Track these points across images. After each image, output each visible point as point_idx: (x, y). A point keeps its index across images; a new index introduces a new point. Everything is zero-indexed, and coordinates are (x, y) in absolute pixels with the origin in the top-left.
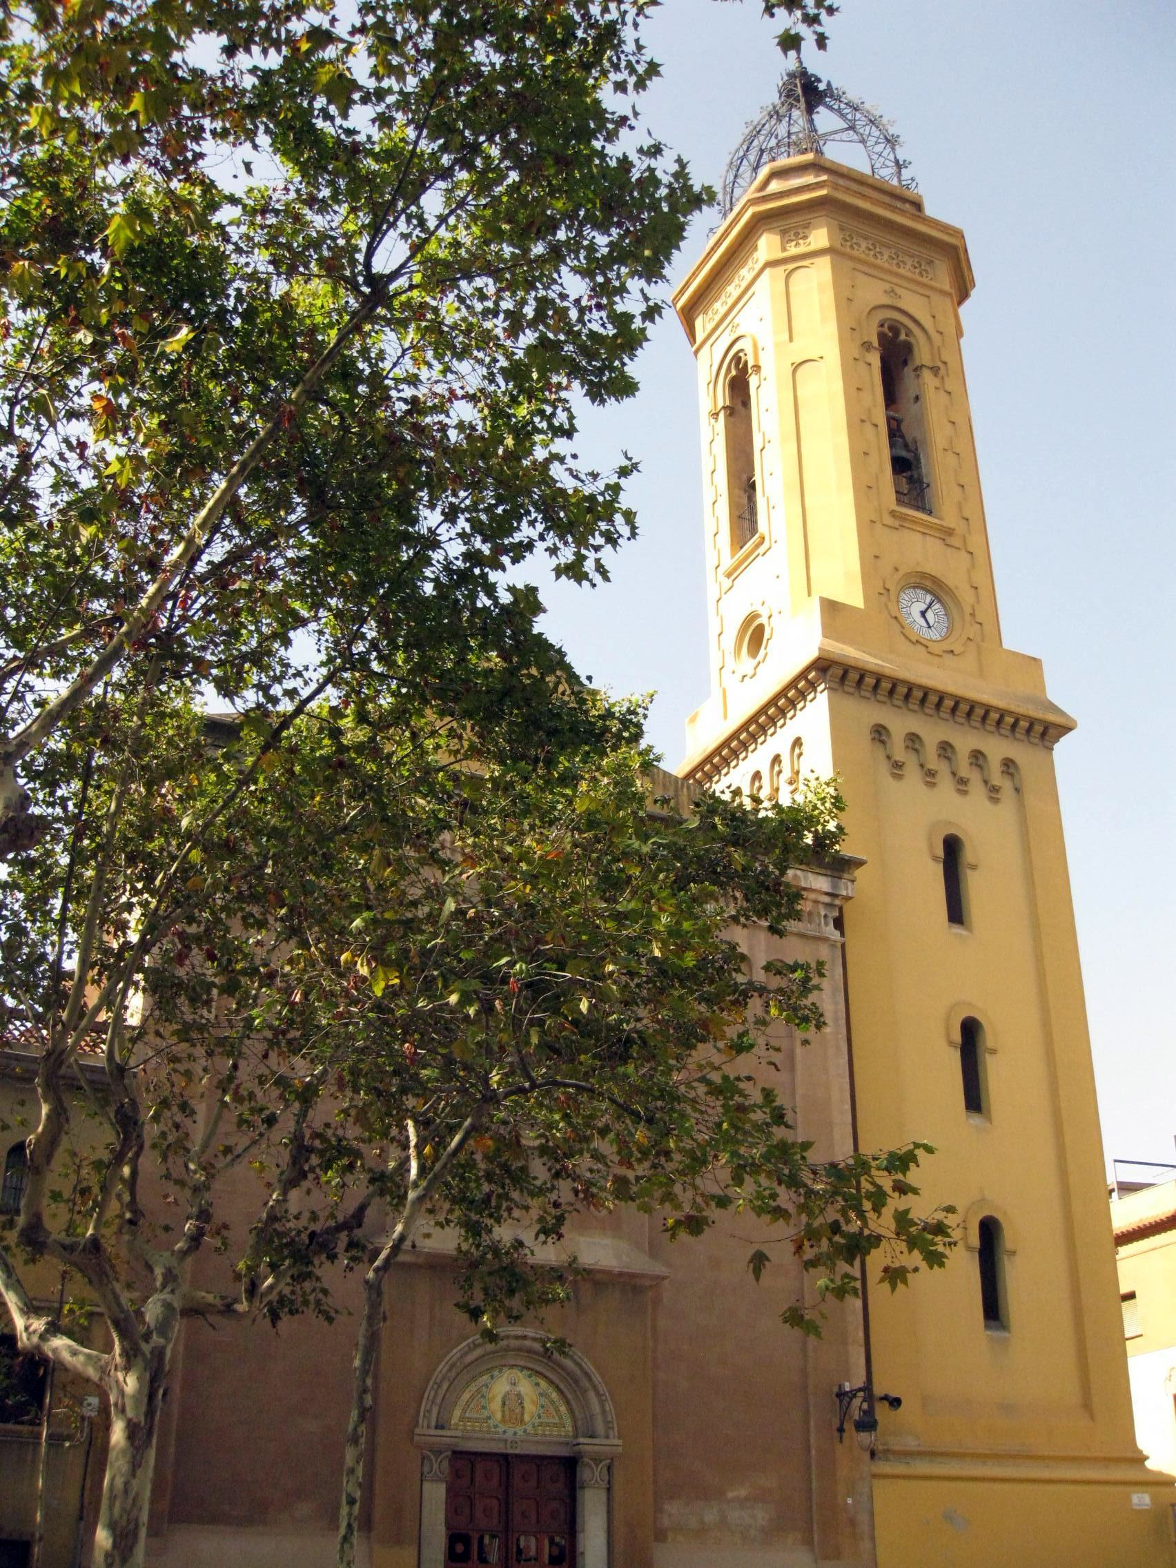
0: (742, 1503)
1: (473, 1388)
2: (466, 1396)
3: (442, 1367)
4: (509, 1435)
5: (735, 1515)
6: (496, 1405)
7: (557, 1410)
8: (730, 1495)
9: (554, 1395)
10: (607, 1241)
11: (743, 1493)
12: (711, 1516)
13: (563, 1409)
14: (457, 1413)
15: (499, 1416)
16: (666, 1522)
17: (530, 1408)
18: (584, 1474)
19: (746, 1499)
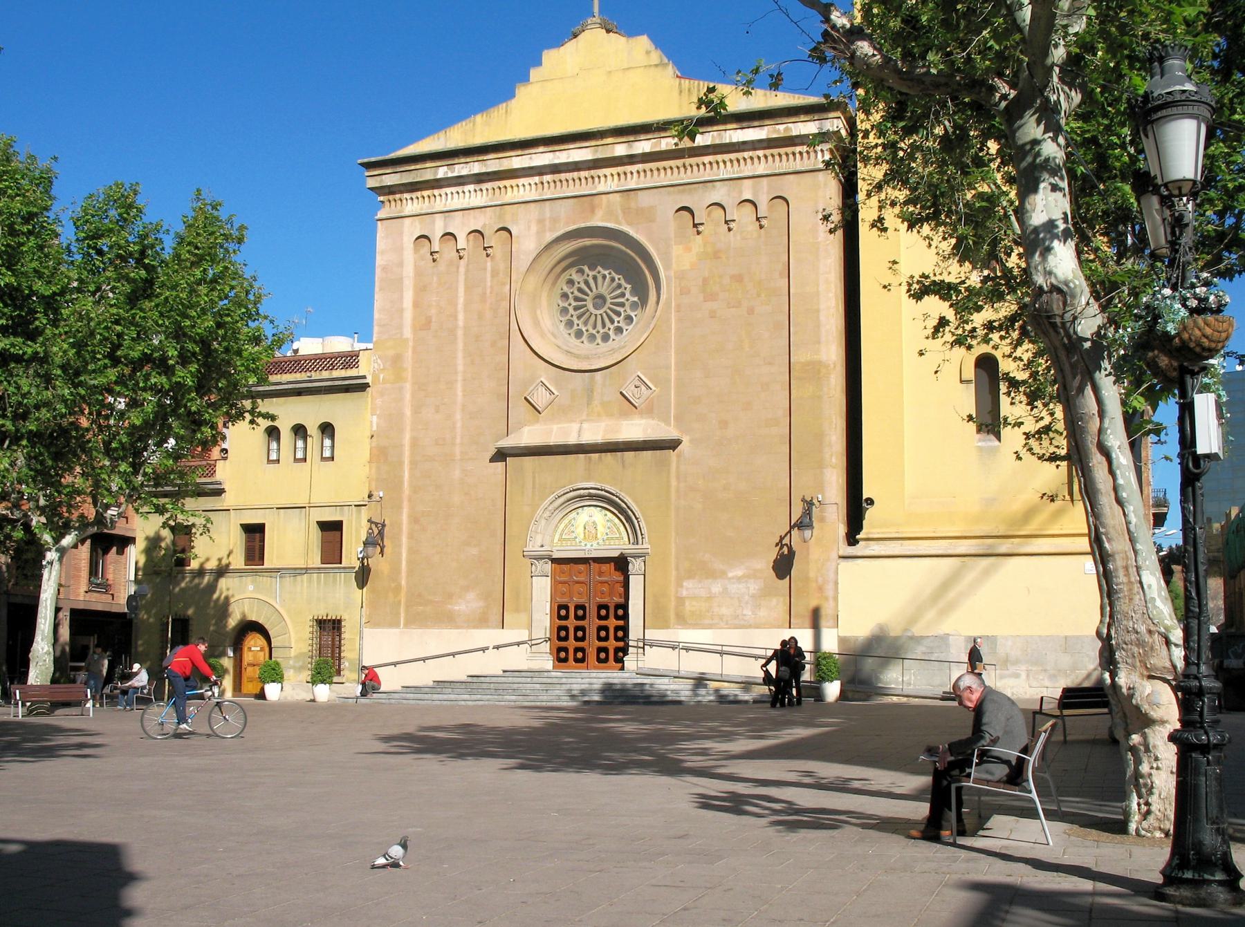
0: (739, 579)
1: (566, 521)
2: (562, 526)
3: (540, 512)
4: (589, 546)
5: (734, 588)
6: (580, 530)
7: (618, 529)
8: (730, 575)
9: (617, 520)
10: (643, 421)
11: (740, 573)
12: (716, 588)
13: (622, 528)
14: (557, 537)
15: (582, 536)
16: (685, 593)
17: (601, 529)
18: (630, 566)
19: (743, 576)
